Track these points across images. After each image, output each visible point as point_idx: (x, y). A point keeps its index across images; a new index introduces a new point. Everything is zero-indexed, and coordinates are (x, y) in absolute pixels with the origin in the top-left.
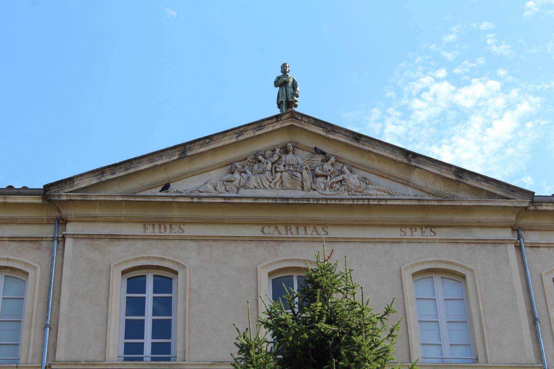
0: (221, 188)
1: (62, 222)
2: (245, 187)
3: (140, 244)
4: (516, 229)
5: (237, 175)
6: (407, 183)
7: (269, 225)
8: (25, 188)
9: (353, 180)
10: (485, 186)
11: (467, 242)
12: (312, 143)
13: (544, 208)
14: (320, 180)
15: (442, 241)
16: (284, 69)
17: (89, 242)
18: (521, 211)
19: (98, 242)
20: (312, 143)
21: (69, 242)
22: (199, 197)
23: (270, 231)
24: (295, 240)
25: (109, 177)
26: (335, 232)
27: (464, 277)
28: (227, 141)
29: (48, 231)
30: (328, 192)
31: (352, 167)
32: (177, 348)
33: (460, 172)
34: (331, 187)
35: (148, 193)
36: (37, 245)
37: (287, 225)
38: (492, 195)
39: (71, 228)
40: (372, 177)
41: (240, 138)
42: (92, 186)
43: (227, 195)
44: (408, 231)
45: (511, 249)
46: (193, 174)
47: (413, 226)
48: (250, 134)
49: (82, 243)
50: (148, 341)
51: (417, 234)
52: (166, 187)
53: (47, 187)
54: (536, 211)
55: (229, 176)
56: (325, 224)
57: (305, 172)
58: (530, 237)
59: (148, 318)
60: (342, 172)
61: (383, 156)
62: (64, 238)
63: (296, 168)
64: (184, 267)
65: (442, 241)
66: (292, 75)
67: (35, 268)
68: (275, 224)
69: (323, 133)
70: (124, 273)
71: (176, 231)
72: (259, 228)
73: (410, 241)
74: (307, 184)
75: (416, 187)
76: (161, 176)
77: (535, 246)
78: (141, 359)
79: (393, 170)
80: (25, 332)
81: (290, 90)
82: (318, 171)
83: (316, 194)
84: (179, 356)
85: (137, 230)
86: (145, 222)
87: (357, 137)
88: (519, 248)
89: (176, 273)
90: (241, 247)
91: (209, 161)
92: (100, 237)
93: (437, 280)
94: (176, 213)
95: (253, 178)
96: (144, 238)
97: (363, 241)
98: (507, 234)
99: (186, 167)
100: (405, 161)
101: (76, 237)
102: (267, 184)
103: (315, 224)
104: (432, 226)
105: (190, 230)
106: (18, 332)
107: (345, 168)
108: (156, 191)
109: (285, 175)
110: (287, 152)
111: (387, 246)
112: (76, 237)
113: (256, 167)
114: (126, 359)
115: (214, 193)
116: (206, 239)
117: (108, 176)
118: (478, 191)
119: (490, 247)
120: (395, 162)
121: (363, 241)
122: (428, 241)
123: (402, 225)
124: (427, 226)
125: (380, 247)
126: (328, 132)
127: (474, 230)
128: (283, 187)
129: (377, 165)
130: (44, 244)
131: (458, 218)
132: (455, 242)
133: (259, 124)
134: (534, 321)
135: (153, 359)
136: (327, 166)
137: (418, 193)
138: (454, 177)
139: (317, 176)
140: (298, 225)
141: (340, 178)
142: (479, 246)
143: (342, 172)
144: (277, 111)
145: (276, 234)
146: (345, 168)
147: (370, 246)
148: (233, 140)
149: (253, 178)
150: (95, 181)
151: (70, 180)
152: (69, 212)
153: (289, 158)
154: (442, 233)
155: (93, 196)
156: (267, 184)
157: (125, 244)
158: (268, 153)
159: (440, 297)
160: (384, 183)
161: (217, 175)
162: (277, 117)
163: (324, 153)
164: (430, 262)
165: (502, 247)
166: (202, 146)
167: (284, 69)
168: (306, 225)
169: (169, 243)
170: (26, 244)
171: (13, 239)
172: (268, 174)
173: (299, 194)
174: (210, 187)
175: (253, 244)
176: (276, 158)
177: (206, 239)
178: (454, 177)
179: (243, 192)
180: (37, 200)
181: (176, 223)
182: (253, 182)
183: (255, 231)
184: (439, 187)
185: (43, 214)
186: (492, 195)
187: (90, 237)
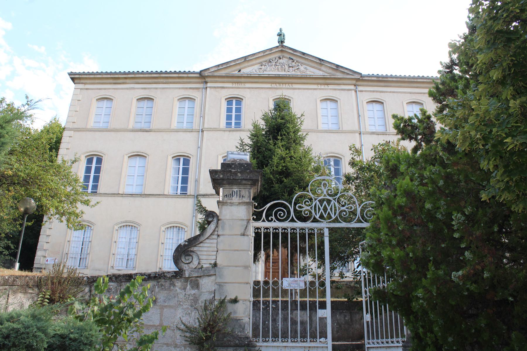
0: (258, 71)
1: (206, 83)
2: (265, 71)
3: (231, 90)
4: (355, 85)
5: (263, 67)
6: (320, 70)
7: (273, 83)
8: (194, 71)
9: (302, 68)
11: (339, 90)
12: (288, 56)
13: (365, 79)
14: (291, 68)
15: (331, 89)
16: (281, 30)
17: (215, 89)
18: (358, 80)
19: (217, 89)
21: (208, 89)
22: (250, 74)
23: (274, 86)
25: (221, 67)
27: (337, 101)
28: (260, 55)
29: (201, 86)
30: (293, 72)
31: (302, 64)
32: (242, 124)
33: (338, 66)
34: (294, 71)
35: (234, 73)
36: (198, 90)
37: (279, 83)
38: (348, 74)
39: (209, 85)
40: (308, 67)
41: (265, 54)
42: (215, 71)
43: (259, 73)
44: (319, 86)
45: (353, 92)
46: (249, 66)
47: (321, 84)
48: (268, 53)
50: (233, 121)
51: (323, 87)
52: (240, 71)
53: (201, 71)
54: (362, 79)
55: (261, 67)
56: (292, 83)
57: (286, 66)
58: (360, 88)
59: (234, 114)
60: (299, 66)
61: (312, 60)
62: (206, 88)
63: (283, 65)
64: (245, 97)
65: (331, 89)
66: (283, 31)
67: (197, 98)
69: (293, 53)
70: (226, 99)
71: (242, 85)
72: (270, 84)
73: (320, 89)
74: (286, 70)
75: (323, 71)
76: (238, 67)
77: (361, 91)
78: (231, 127)
79: (316, 65)
80: (195, 118)
81: (282, 37)
82: (290, 65)
83: (289, 73)
84: (243, 126)
85: (230, 85)
86: (233, 83)
87: (304, 54)
88: (356, 91)
89: (243, 99)
90: (264, 91)
91: (254, 62)
92: (218, 87)
93: (328, 102)
94: (243, 80)
95: (268, 68)
96: (232, 88)
98: (352, 87)
99: (246, 64)
100: (320, 62)
101: (210, 87)
102: (273, 70)
103: (289, 83)
105: (248, 85)
106: (193, 118)
107: (299, 64)
108: (236, 72)
110: (280, 59)
111: (312, 91)
112: (210, 87)
113: (270, 63)
114: (226, 127)
115: (256, 73)
116: (252, 88)
117: (221, 67)
119: (346, 91)
120: (316, 62)
122: (326, 89)
123: (318, 84)
124: (326, 84)
125: (310, 91)
126: (294, 52)
127: (342, 86)
128: (278, 71)
129: (311, 64)
130: (200, 90)
131: (337, 82)
132: (335, 89)
133: (271, 49)
134: (359, 116)
135: (235, 127)
136: (293, 64)
137: (324, 73)
138: (335, 68)
139: (290, 67)
140: (283, 83)
141: (298, 68)
142: (342, 91)
143: (299, 66)
144: (278, 45)
145: (276, 87)
146: (299, 64)
147: (306, 91)
148: (262, 55)
149: (268, 68)
150: (216, 69)
151: (208, 69)
152: (207, 80)
153: (281, 61)
154: (331, 87)
155: (216, 74)
156: (273, 70)
157: (226, 90)
158: (274, 59)
159: (329, 108)
160: (312, 70)
161: (257, 67)
162: (277, 47)
163: (292, 59)
164: (326, 96)
165: (350, 92)
166: (251, 57)
167: (281, 30)
168: (285, 83)
169: (240, 89)
170: (195, 90)
171: (190, 88)
172: (273, 66)
173: (283, 73)
174: (254, 71)
175: (268, 90)
176: (276, 61)
177: (252, 88)
178: (335, 68)
179: (265, 73)
180: (198, 75)
181: (243, 83)
182: (268, 69)
183: (269, 86)
184: (330, 71)
187: (215, 87)
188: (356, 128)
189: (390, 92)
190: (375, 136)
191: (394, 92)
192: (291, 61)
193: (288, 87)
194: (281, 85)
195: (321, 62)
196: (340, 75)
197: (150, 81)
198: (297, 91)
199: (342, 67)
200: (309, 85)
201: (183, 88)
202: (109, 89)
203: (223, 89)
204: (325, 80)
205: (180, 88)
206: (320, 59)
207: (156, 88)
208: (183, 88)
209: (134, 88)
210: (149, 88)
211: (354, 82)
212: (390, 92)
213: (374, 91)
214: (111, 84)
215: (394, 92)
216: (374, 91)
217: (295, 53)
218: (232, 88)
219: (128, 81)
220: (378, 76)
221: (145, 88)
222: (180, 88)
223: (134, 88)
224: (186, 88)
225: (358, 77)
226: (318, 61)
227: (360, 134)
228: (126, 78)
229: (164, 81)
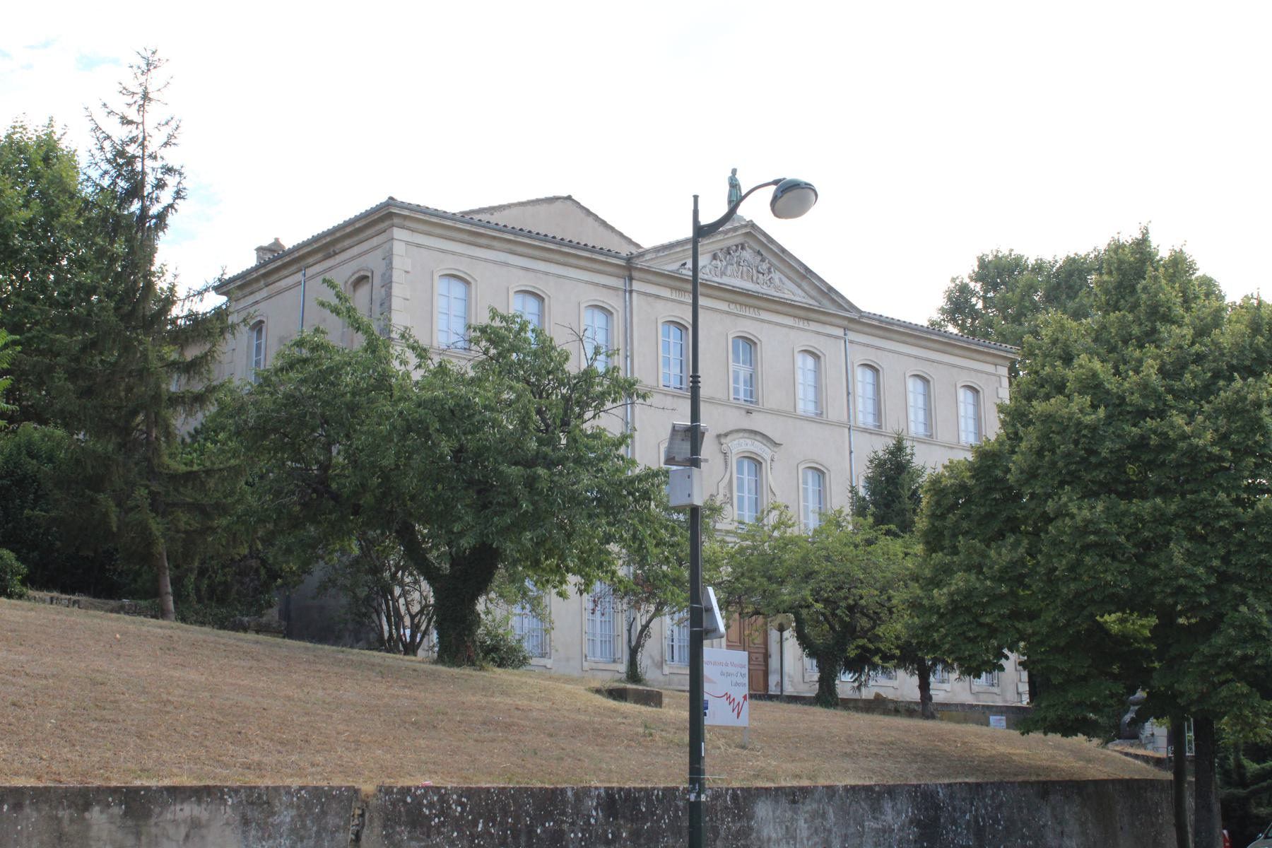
1: (631, 279)
6: (799, 286)
10: (840, 301)
18: (851, 320)
19: (650, 299)
21: (634, 295)
24: (744, 317)
26: (765, 315)
29: (619, 283)
31: (777, 269)
33: (831, 289)
37: (741, 304)
38: (840, 306)
39: (636, 285)
47: (799, 318)
49: (642, 297)
51: (801, 325)
56: (759, 308)
58: (851, 336)
62: (631, 292)
68: (735, 303)
73: (799, 329)
75: (803, 290)
77: (851, 342)
86: (672, 288)
96: (673, 300)
97: (777, 324)
98: (840, 332)
101: (639, 292)
103: (754, 307)
104: (808, 320)
109: (745, 269)
112: (639, 292)
118: (834, 301)
120: (798, 271)
121: (777, 324)
125: (785, 330)
127: (828, 327)
129: (786, 270)
134: (848, 394)
152: (635, 274)
157: (663, 302)
167: (734, 171)
168: (750, 307)
170: (611, 291)
175: (725, 315)
185: (621, 272)
186: (840, 306)
188: (845, 418)
189: (890, 351)
190: (867, 435)
191: (894, 352)
194: (738, 306)
195: (804, 274)
198: (766, 325)
199: (836, 292)
200: (782, 316)
202: (462, 255)
203: (658, 301)
204: (805, 313)
205: (587, 282)
206: (807, 269)
207: (547, 274)
209: (507, 264)
210: (533, 270)
211: (845, 323)
212: (890, 351)
214: (462, 242)
215: (894, 352)
218: (673, 300)
219: (495, 244)
220: (880, 318)
221: (527, 269)
222: (587, 282)
223: (507, 264)
224: (597, 284)
225: (854, 315)
226: (802, 271)
228: (494, 238)
229: (562, 259)
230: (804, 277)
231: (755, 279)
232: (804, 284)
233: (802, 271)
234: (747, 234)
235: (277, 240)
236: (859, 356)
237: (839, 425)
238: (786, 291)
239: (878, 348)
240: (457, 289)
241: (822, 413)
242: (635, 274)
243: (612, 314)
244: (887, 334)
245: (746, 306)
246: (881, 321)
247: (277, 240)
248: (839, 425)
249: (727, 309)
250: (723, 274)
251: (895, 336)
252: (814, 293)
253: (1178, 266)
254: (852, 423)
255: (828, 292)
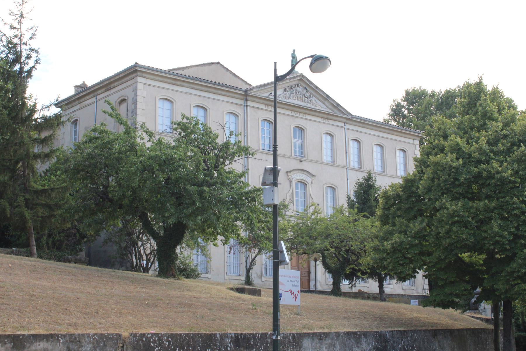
1: (247, 100)
6: (324, 104)
10: (342, 110)
12: (305, 86)
15: (330, 124)
19: (255, 109)
20: (305, 86)
21: (248, 108)
26: (308, 117)
29: (241, 102)
31: (313, 95)
33: (338, 104)
37: (297, 112)
38: (342, 113)
39: (249, 103)
49: (252, 108)
51: (325, 121)
58: (347, 126)
62: (247, 106)
65: (330, 124)
68: (295, 111)
77: (348, 129)
79: (321, 99)
86: (266, 104)
92: (256, 108)
96: (266, 110)
97: (314, 121)
101: (250, 106)
103: (303, 113)
104: (328, 119)
118: (340, 110)
119: (339, 128)
120: (323, 97)
121: (314, 121)
122: (327, 124)
125: (317, 124)
127: (337, 122)
129: (318, 96)
131: (334, 118)
134: (346, 153)
142: (337, 127)
147: (315, 123)
154: (330, 122)
157: (261, 111)
167: (294, 51)
168: (301, 113)
170: (238, 106)
180: (243, 93)
186: (342, 113)
189: (365, 133)
190: (355, 171)
191: (367, 134)
192: (305, 91)
193: (303, 117)
194: (296, 113)
195: (326, 98)
196: (339, 114)
197: (203, 88)
198: (308, 121)
199: (341, 106)
200: (316, 117)
201: (229, 102)
202: (169, 89)
205: (226, 102)
206: (327, 96)
207: (208, 98)
208: (229, 102)
209: (190, 94)
210: (202, 96)
211: (345, 120)
212: (365, 133)
213: (355, 131)
214: (169, 83)
215: (367, 134)
216: (355, 131)
217: (310, 85)
218: (266, 110)
219: (185, 84)
220: (361, 118)
221: (199, 96)
222: (226, 102)
223: (190, 94)
224: (231, 103)
225: (349, 117)
226: (325, 97)
227: (347, 169)
228: (184, 81)
229: (215, 91)
230: (326, 99)
231: (303, 100)
232: (326, 103)
233: (325, 97)
234: (300, 80)
235: (84, 82)
236: (351, 135)
237: (342, 167)
238: (318, 106)
239: (360, 132)
240: (167, 105)
241: (334, 162)
242: (249, 98)
243: (238, 116)
244: (364, 125)
245: (299, 112)
246: (361, 120)
247: (84, 82)
248: (342, 167)
249: (291, 114)
250: (289, 98)
251: (368, 126)
252: (331, 107)
253: (496, 94)
254: (348, 166)
255: (337, 106)
